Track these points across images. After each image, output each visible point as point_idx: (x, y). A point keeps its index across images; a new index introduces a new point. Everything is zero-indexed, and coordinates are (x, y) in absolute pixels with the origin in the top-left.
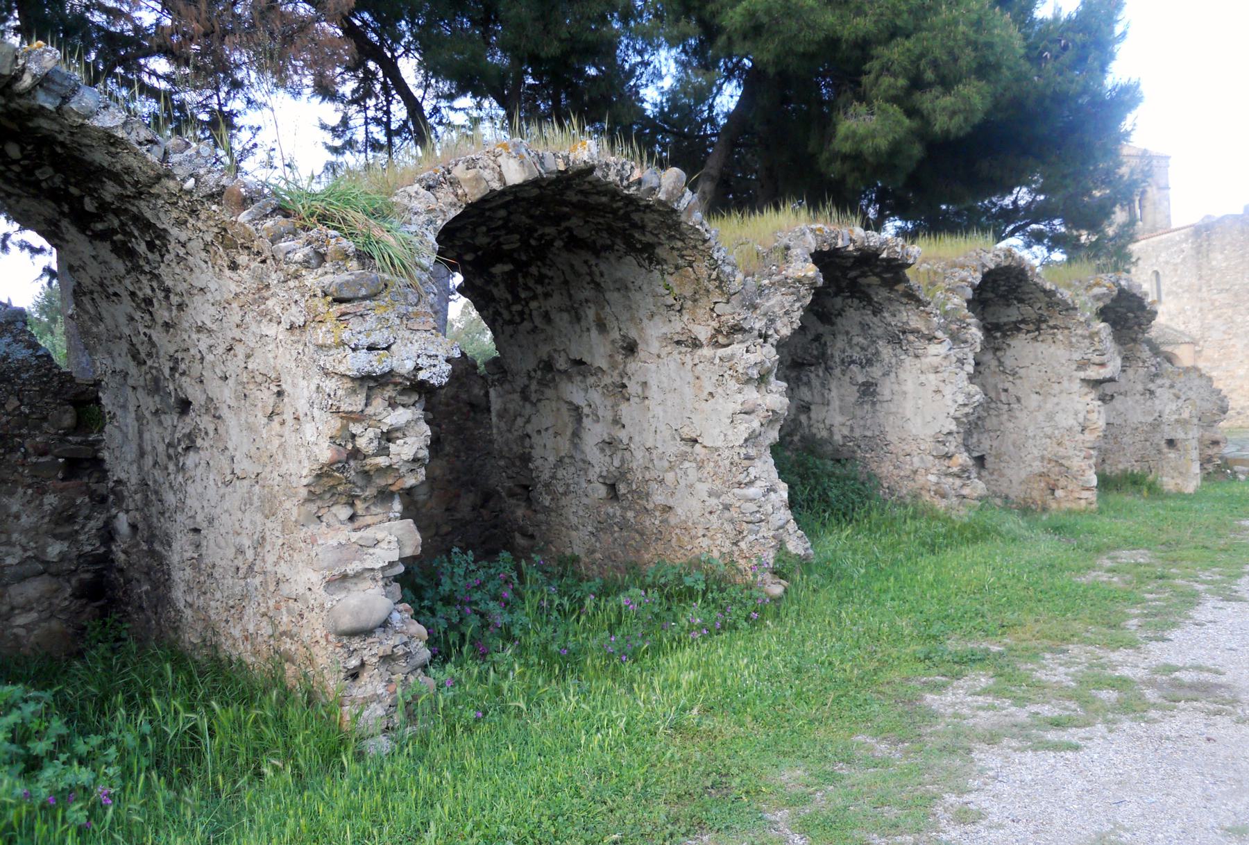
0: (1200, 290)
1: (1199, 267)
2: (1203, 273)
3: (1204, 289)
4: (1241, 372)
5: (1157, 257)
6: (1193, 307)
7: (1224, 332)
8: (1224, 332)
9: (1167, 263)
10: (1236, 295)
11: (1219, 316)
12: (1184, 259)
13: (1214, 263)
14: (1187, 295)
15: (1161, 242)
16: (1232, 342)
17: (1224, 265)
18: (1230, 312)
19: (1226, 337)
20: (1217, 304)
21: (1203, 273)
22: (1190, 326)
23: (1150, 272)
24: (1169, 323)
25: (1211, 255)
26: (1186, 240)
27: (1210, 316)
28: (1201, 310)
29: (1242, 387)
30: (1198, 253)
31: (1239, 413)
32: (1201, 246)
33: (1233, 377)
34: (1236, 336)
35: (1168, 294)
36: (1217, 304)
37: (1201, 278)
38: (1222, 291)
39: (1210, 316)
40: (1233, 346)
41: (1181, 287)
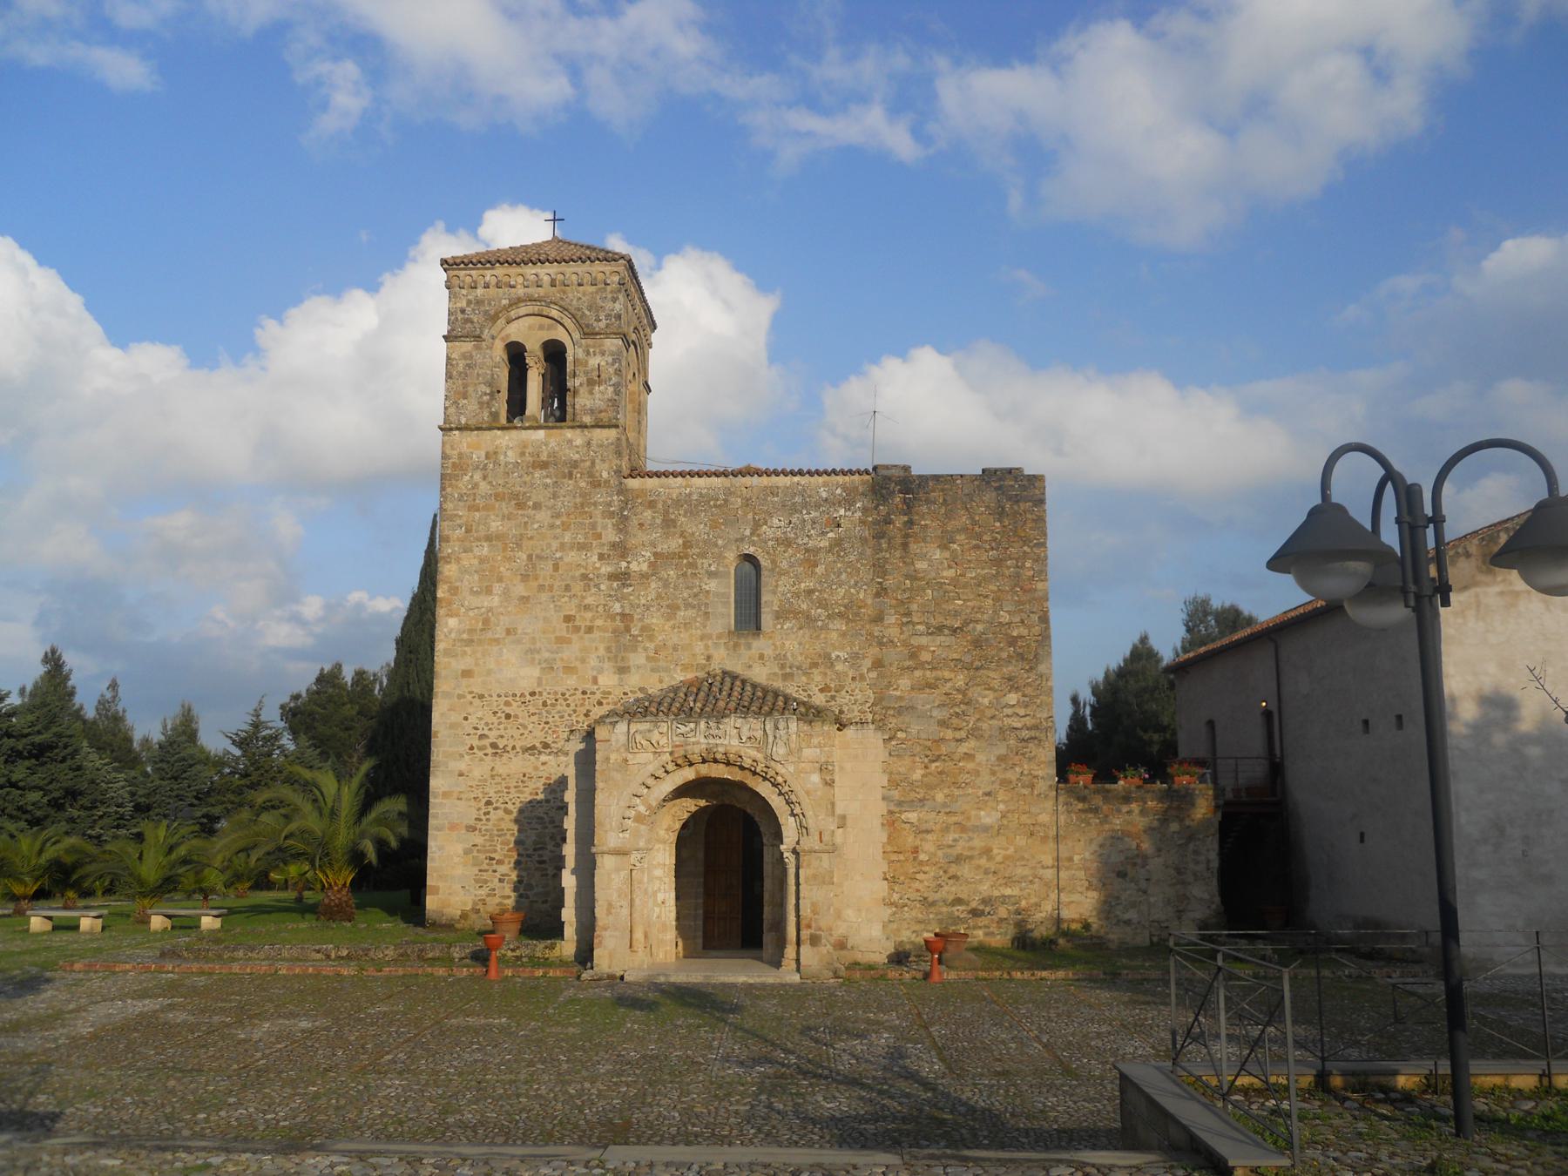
0: (878, 619)
1: (880, 568)
2: (890, 582)
3: (891, 619)
4: (988, 817)
5: (756, 525)
6: (855, 658)
7: (943, 724)
8: (943, 724)
9: (787, 543)
10: (977, 643)
11: (930, 686)
12: (838, 543)
13: (921, 565)
14: (839, 625)
15: (773, 491)
16: (964, 748)
17: (950, 573)
18: (960, 680)
19: (949, 734)
20: (925, 656)
21: (890, 582)
22: (843, 699)
23: (731, 557)
24: (778, 684)
25: (913, 547)
26: (849, 503)
27: (905, 682)
28: (878, 664)
29: (987, 852)
30: (879, 536)
31: (975, 913)
32: (889, 522)
33: (962, 828)
34: (975, 733)
35: (779, 616)
36: (925, 656)
37: (882, 592)
38: (940, 629)
39: (905, 682)
40: (969, 756)
41: (822, 604)
